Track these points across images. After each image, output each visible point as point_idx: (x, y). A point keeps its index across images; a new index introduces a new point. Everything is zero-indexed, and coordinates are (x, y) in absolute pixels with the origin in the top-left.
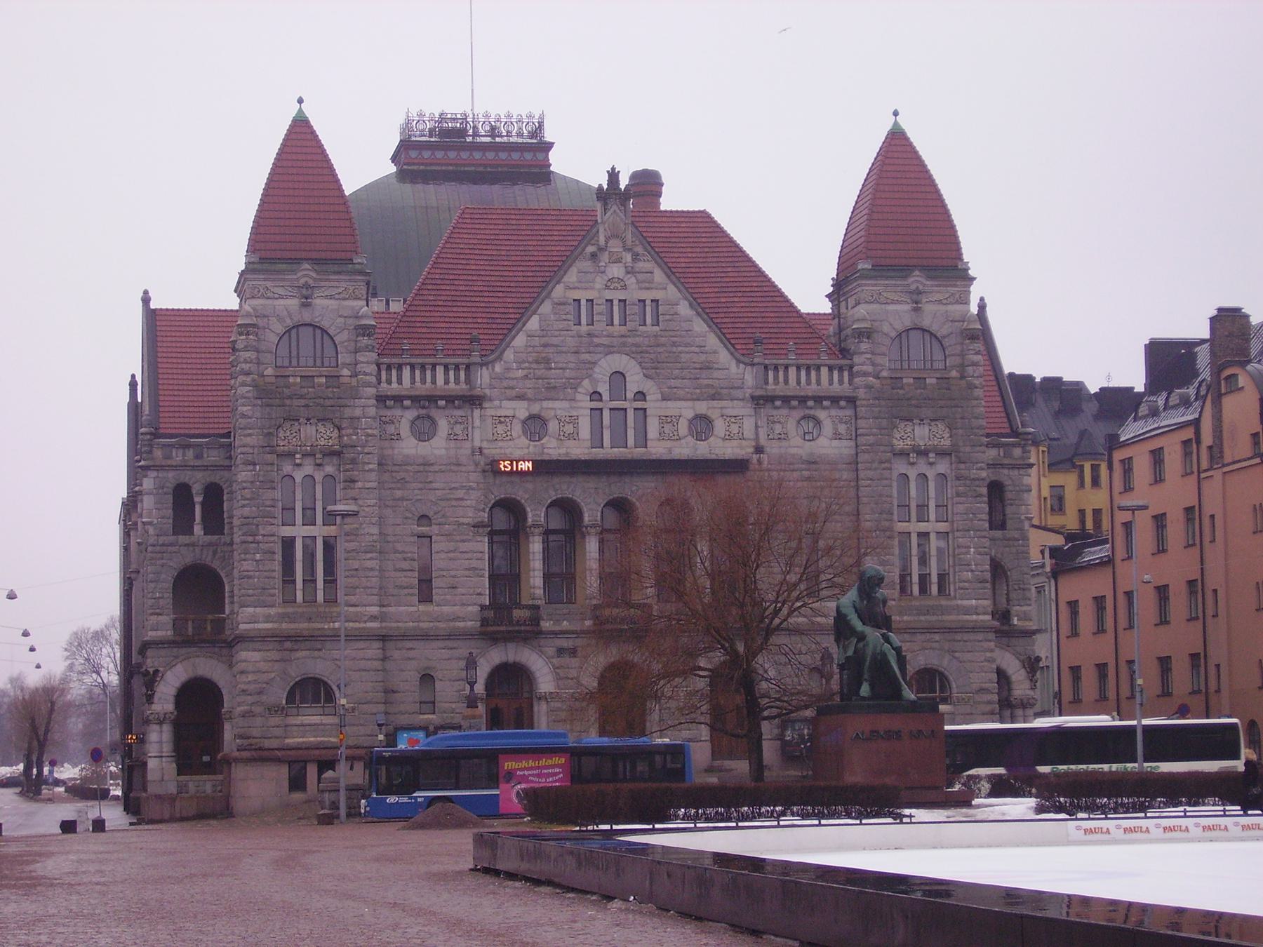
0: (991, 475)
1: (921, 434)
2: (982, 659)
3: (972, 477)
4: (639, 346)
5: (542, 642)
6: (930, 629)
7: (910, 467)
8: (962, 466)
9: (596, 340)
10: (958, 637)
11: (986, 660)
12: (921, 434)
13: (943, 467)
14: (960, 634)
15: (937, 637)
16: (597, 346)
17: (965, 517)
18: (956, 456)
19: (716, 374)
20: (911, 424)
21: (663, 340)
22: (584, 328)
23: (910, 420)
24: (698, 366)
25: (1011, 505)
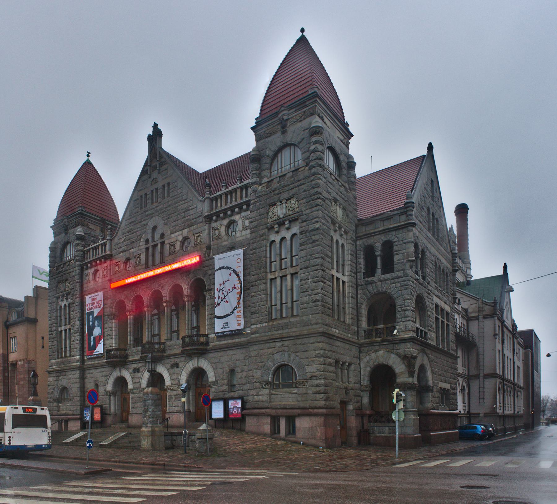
0: (383, 238)
1: (280, 211)
2: (314, 355)
3: (310, 229)
4: (162, 209)
5: (128, 366)
6: (282, 339)
7: (276, 235)
8: (304, 224)
9: (147, 213)
10: (299, 341)
11: (316, 356)
12: (280, 211)
13: (295, 229)
14: (300, 340)
15: (286, 343)
16: (147, 215)
17: (305, 258)
18: (300, 219)
19: (191, 212)
20: (276, 207)
21: (170, 203)
22: (143, 208)
23: (275, 205)
24: (183, 211)
25: (397, 254)
